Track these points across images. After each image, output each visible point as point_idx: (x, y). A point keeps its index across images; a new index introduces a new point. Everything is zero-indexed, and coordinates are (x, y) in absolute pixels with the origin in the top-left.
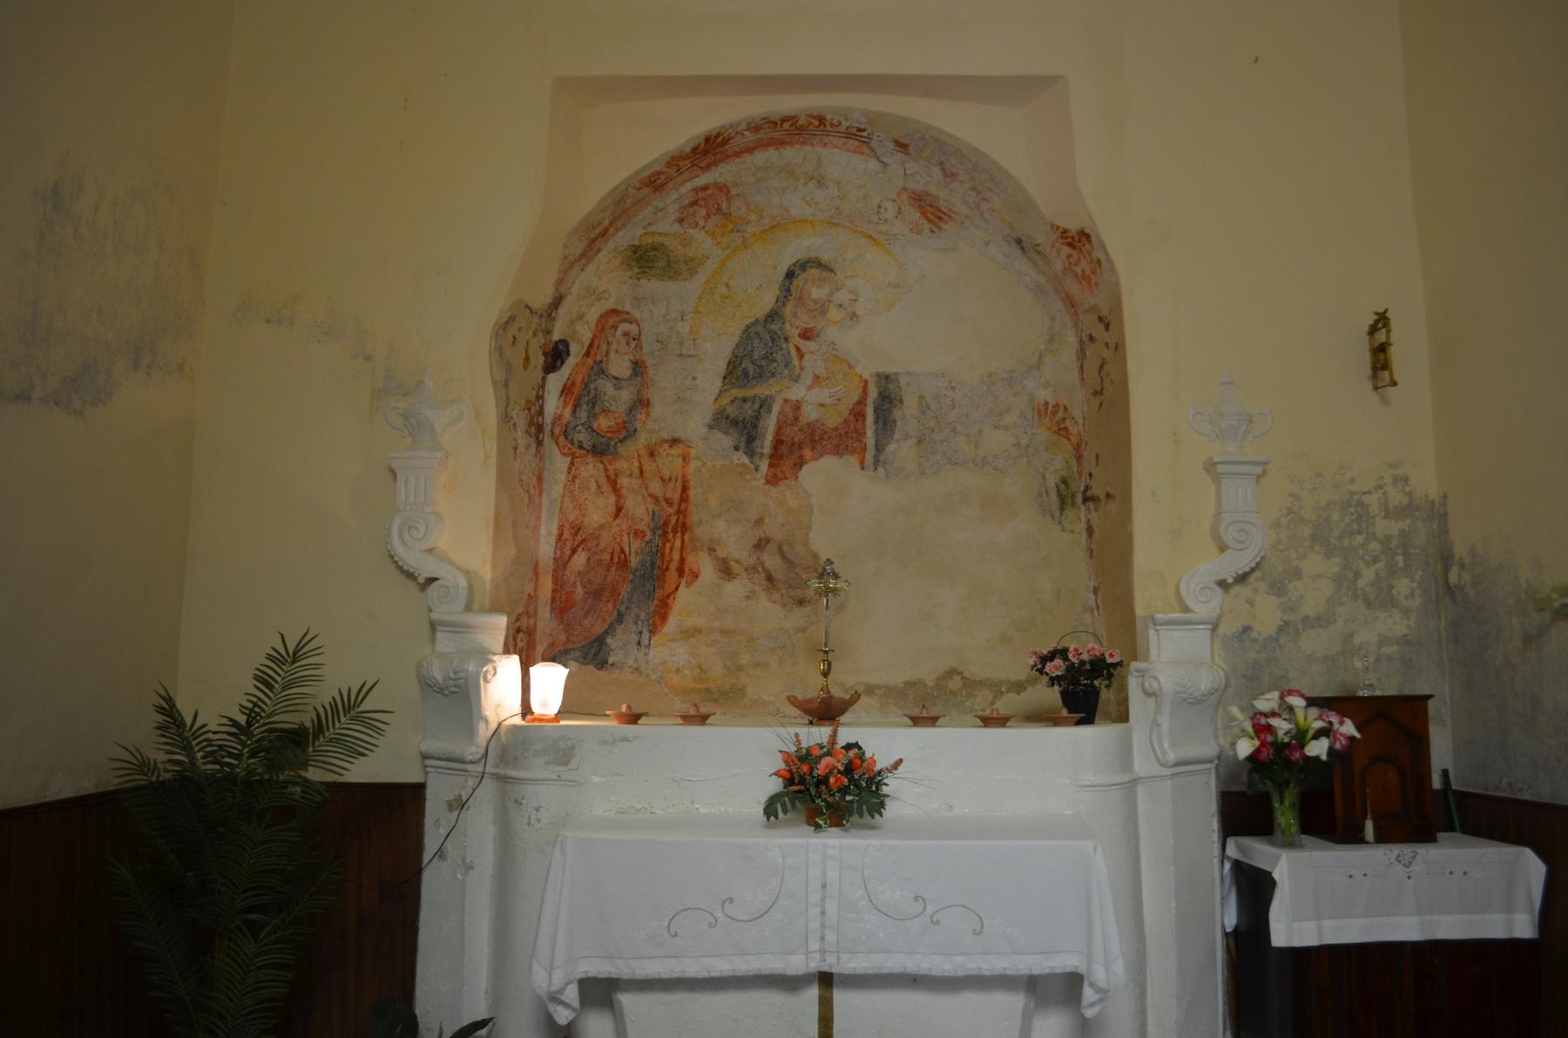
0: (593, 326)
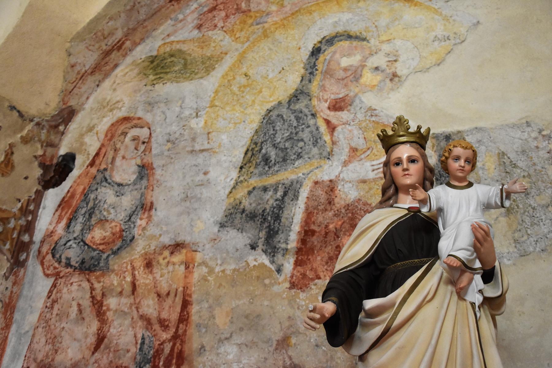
0: (102, 136)
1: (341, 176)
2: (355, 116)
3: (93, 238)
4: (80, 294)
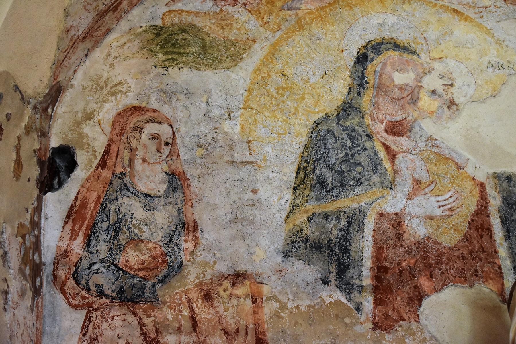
0: (108, 129)
1: (407, 209)
2: (416, 144)
3: (127, 261)
4: (126, 331)
